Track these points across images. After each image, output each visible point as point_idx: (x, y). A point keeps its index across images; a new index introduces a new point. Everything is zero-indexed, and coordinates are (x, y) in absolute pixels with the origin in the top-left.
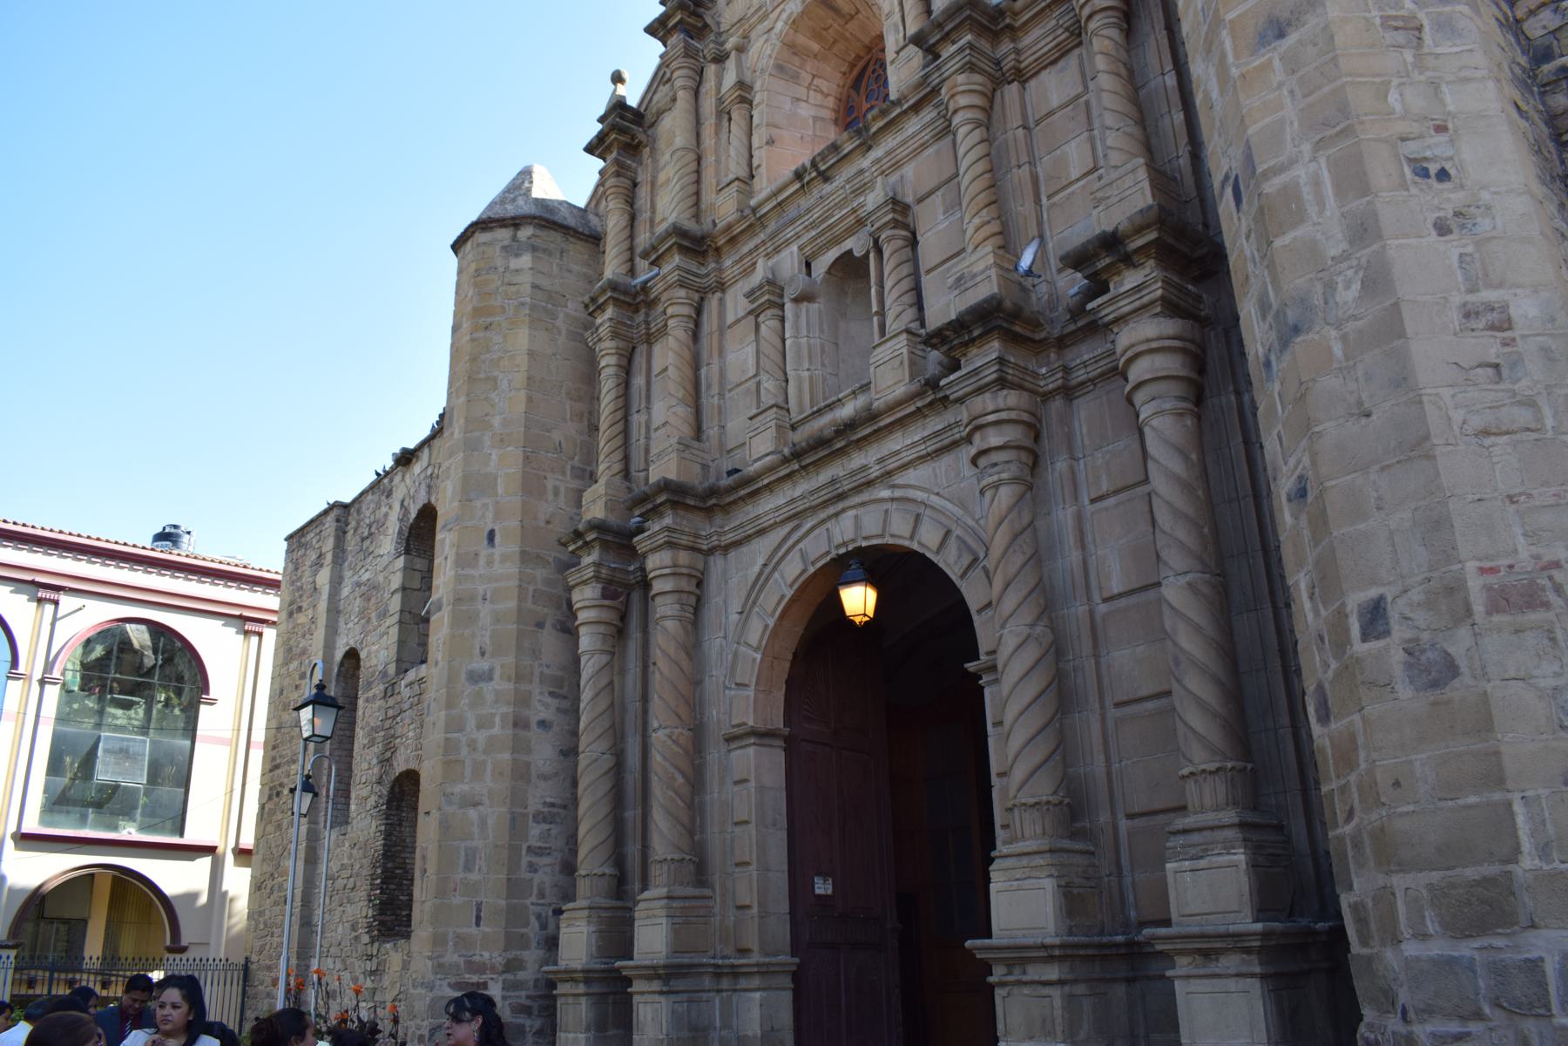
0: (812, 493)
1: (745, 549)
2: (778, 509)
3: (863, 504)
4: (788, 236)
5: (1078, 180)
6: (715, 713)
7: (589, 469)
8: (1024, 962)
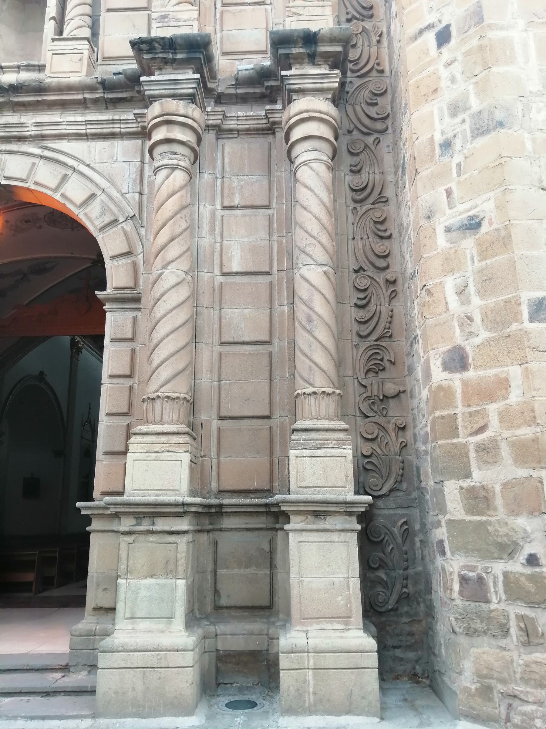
5: (249, 4)
8: (154, 516)
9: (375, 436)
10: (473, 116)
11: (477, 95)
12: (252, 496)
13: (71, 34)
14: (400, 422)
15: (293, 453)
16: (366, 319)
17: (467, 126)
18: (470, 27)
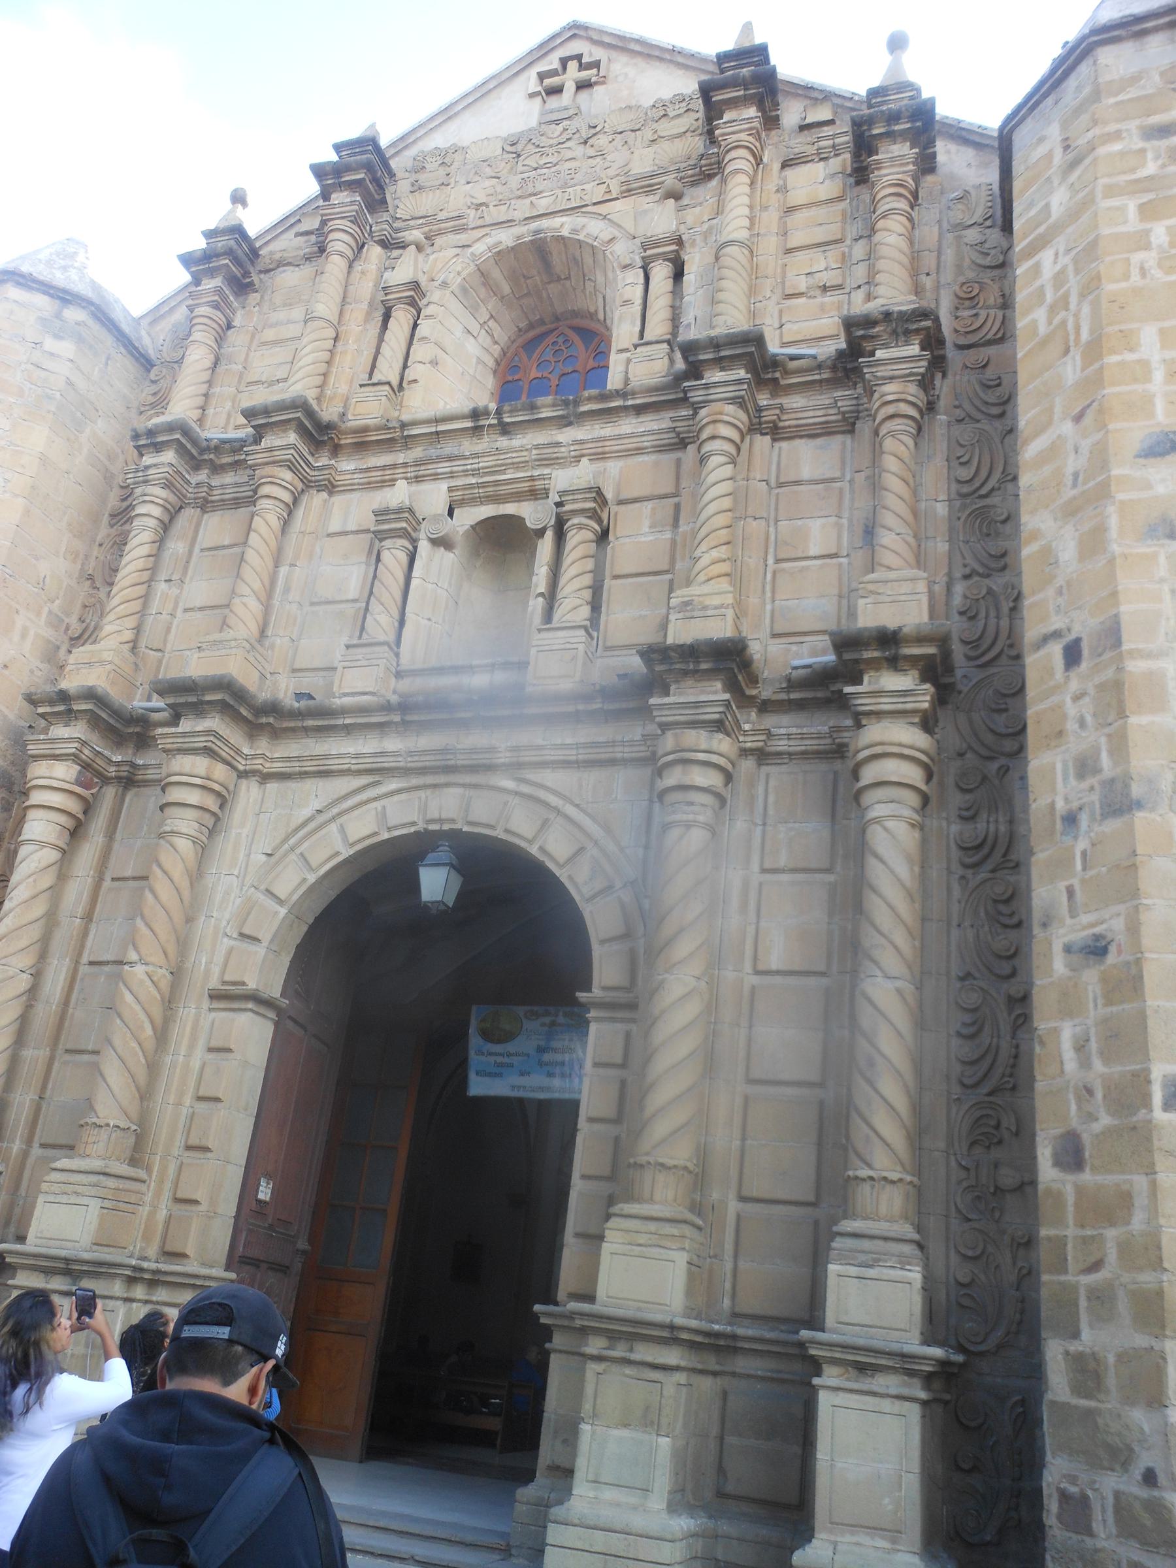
0: (411, 753)
1: (292, 785)
2: (358, 756)
3: (475, 786)
4: (439, 471)
5: (815, 558)
6: (204, 961)
7: (67, 620)
8: (633, 1338)
9: (978, 1252)
10: (1104, 783)
11: (1111, 753)
12: (783, 1327)
13: (563, 619)
14: (1020, 1233)
15: (832, 1268)
16: (976, 1057)
17: (1095, 797)
18: (1104, 650)
